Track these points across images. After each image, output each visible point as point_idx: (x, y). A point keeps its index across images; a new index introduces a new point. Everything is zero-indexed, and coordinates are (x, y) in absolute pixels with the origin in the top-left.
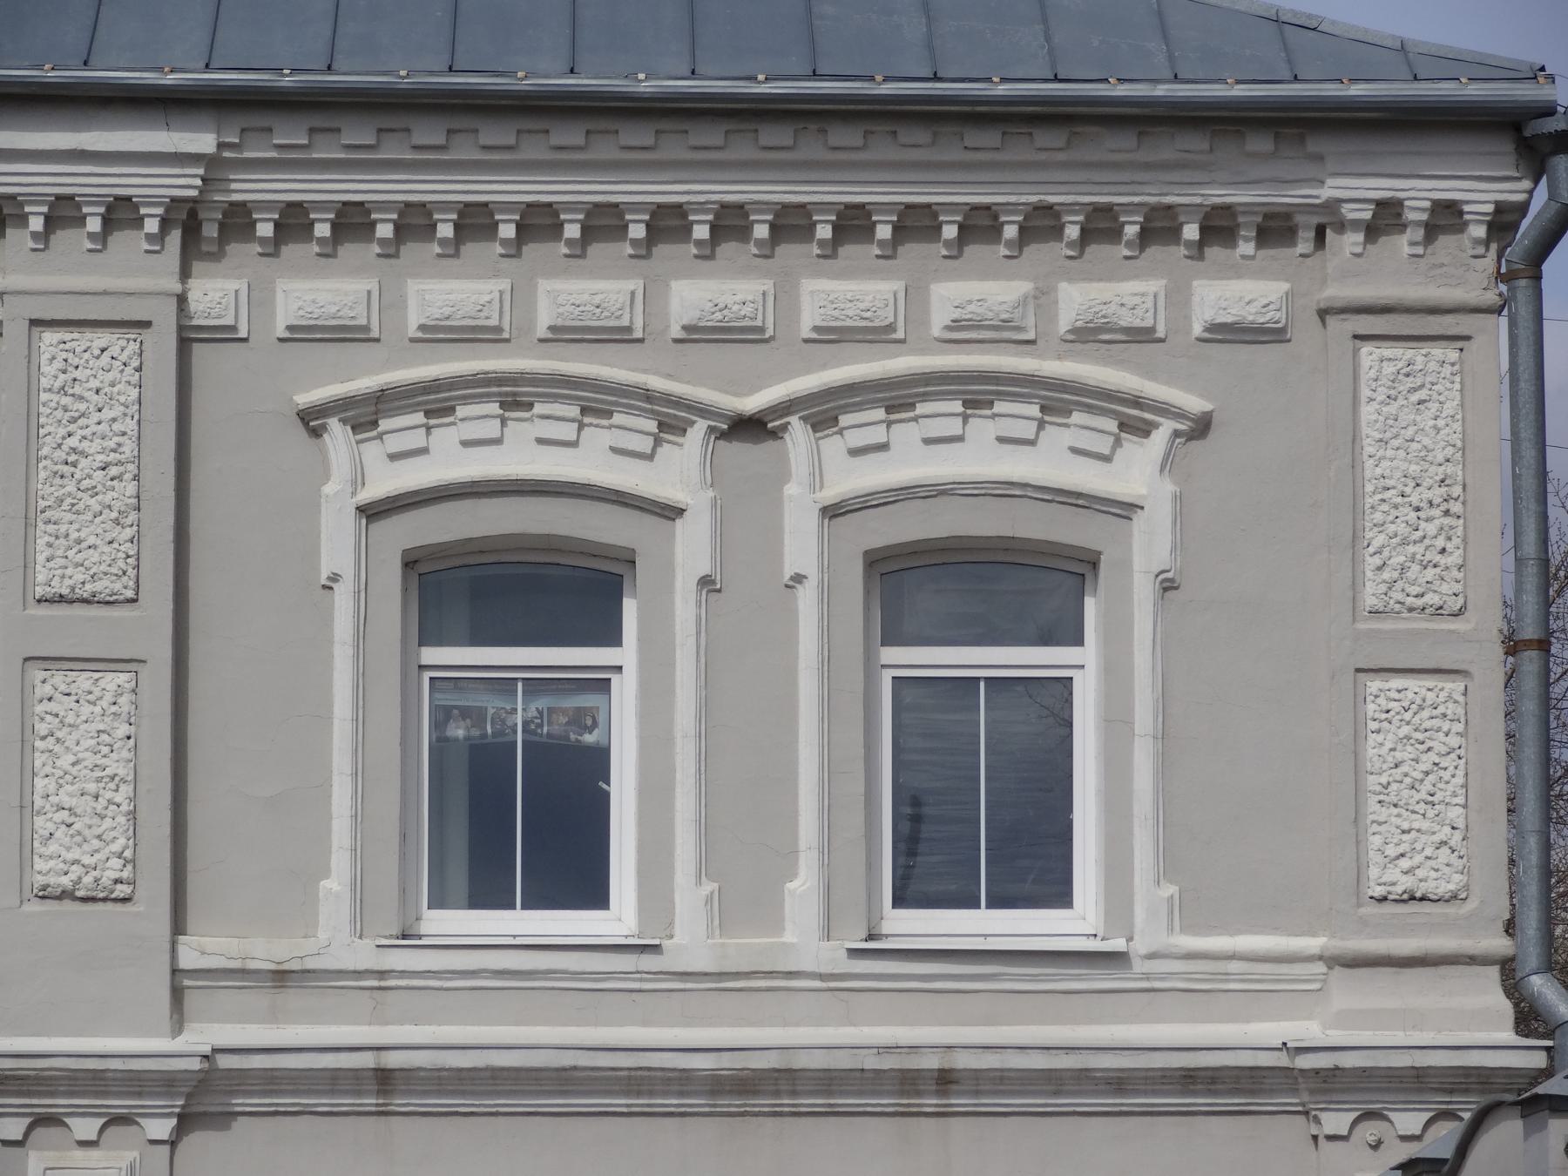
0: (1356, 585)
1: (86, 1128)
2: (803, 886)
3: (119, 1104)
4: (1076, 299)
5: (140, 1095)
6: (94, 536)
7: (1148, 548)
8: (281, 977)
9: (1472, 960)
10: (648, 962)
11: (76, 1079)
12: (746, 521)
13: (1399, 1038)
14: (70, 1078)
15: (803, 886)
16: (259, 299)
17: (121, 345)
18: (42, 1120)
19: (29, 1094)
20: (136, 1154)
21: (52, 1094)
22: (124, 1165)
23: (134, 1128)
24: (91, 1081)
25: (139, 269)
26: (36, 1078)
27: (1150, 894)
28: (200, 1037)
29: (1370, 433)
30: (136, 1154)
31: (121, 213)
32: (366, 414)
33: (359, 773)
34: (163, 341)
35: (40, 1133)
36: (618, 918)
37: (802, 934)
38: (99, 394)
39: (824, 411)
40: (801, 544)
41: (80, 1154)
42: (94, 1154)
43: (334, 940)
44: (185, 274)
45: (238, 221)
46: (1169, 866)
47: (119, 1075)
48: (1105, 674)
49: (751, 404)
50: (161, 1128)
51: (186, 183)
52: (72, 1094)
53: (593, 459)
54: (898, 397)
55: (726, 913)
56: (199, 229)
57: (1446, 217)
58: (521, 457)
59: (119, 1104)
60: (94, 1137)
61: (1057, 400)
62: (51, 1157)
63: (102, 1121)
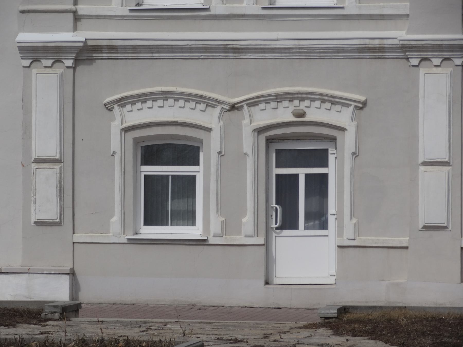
1: (437, 61)
3: (446, 54)
5: (452, 51)
11: (434, 47)
14: (432, 47)
18: (424, 59)
19: (420, 51)
20: (451, 69)
21: (427, 51)
22: (448, 72)
23: (451, 62)
24: (438, 47)
26: (422, 47)
30: (451, 69)
35: (423, 63)
41: (435, 69)
42: (439, 69)
47: (447, 46)
52: (433, 51)
59: (446, 54)
60: (439, 64)
62: (426, 70)
63: (441, 59)
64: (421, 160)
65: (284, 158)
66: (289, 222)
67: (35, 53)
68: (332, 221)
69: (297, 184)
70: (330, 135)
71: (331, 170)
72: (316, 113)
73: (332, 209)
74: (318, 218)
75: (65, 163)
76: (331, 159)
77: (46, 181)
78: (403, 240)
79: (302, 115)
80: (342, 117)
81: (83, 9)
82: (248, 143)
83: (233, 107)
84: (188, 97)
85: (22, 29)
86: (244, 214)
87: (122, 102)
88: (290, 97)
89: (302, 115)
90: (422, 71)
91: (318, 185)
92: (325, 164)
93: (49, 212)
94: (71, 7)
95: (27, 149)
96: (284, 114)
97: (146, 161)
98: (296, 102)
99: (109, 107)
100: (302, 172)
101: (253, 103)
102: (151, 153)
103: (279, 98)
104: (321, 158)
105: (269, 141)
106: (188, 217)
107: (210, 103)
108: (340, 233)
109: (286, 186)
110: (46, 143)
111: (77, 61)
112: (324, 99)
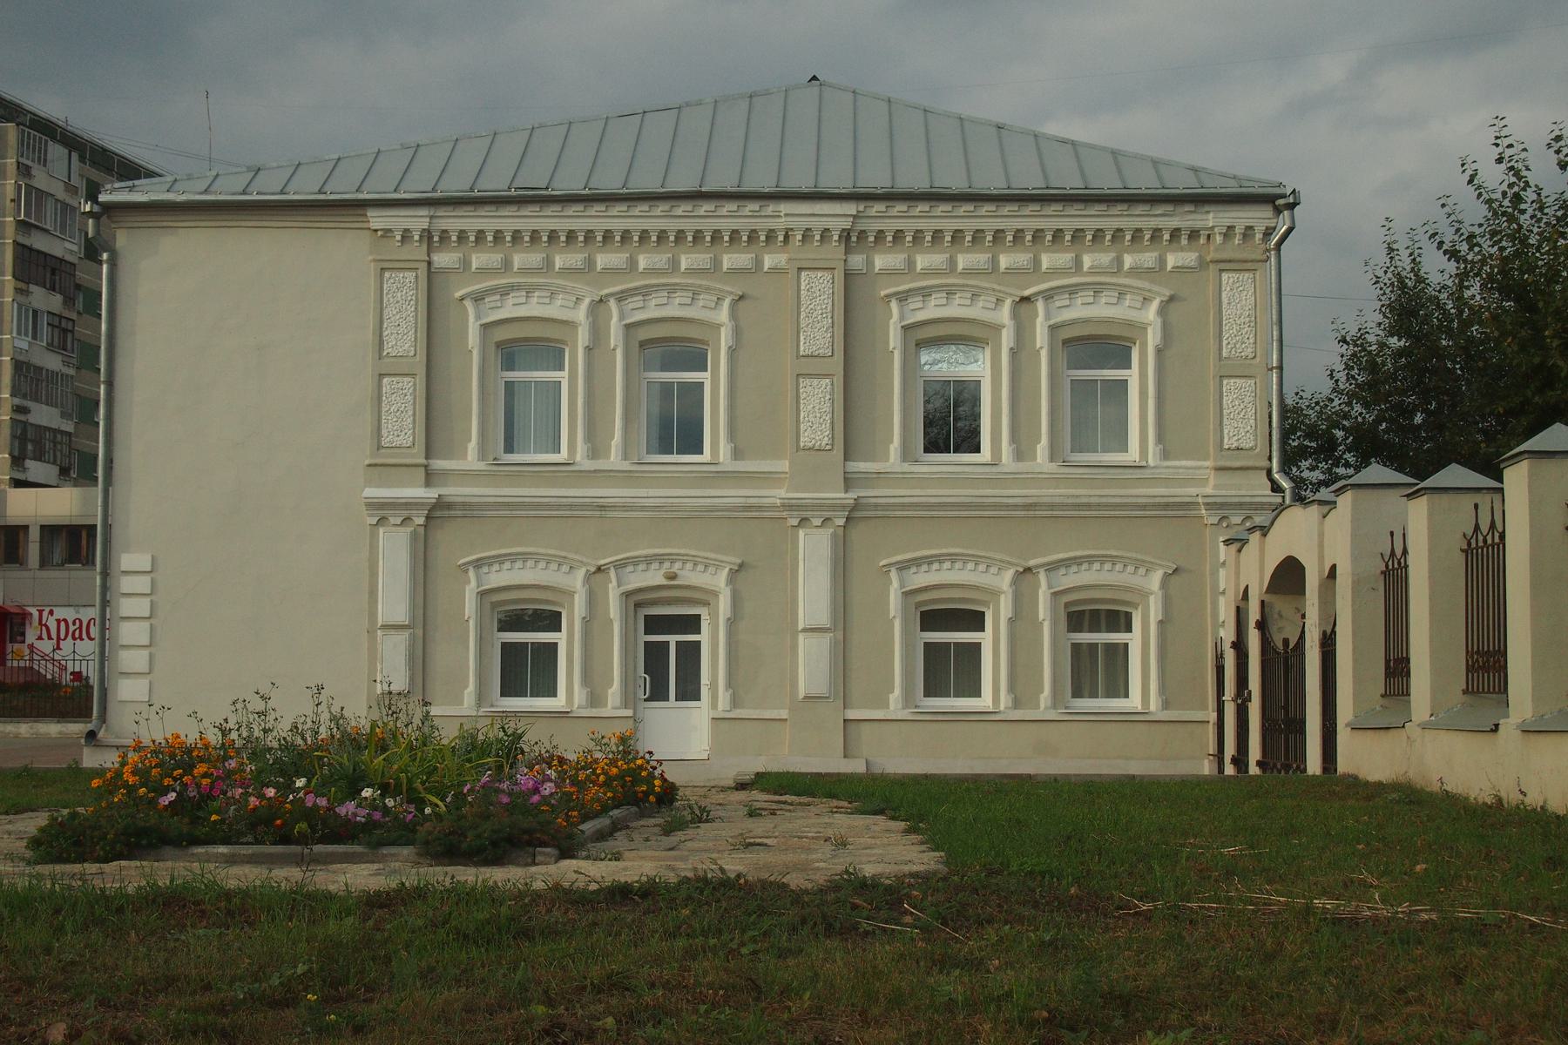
0: (1220, 349)
3: (827, 514)
6: (818, 333)
9: (1256, 468)
10: (994, 469)
13: (1233, 493)
17: (827, 275)
29: (1225, 301)
34: (839, 275)
39: (1048, 295)
44: (846, 253)
45: (862, 234)
49: (1027, 293)
51: (846, 224)
54: (1072, 290)
55: (1019, 455)
57: (1248, 231)
58: (953, 311)
64: (801, 626)
65: (653, 624)
67: (382, 510)
68: (704, 691)
71: (704, 637)
74: (689, 692)
76: (704, 625)
78: (784, 714)
81: (439, 464)
85: (369, 483)
88: (660, 558)
89: (673, 577)
91: (690, 654)
94: (423, 461)
95: (373, 615)
96: (655, 577)
97: (505, 626)
98: (667, 565)
99: (464, 569)
100: (672, 639)
103: (649, 560)
104: (693, 624)
105: (638, 605)
108: (714, 705)
109: (655, 654)
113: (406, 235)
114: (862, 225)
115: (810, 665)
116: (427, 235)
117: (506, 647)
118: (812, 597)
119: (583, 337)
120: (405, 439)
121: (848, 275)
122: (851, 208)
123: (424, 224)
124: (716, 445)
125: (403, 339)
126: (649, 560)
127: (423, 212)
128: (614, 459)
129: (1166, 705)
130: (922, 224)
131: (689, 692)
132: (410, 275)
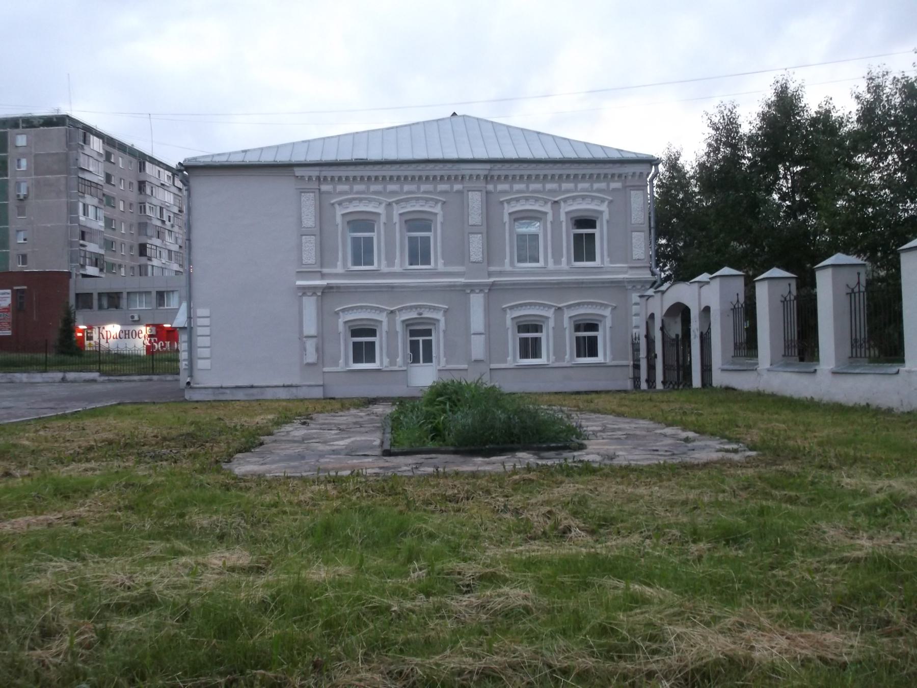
2: (564, 259)
4: (596, 186)
7: (606, 216)
8: (501, 272)
12: (556, 214)
15: (564, 259)
16: (495, 187)
17: (479, 193)
25: (481, 184)
27: (606, 259)
28: (492, 280)
31: (478, 176)
32: (509, 201)
33: (511, 247)
36: (541, 263)
37: (564, 265)
38: (475, 200)
39: (565, 200)
40: (563, 217)
43: (507, 267)
45: (492, 177)
46: (609, 256)
48: (600, 233)
50: (487, 291)
51: (486, 172)
53: (536, 207)
56: (488, 178)
61: (593, 198)
66: (416, 360)
67: (305, 290)
68: (434, 359)
69: (420, 345)
70: (435, 322)
71: (433, 338)
72: (427, 314)
73: (434, 355)
74: (428, 358)
75: (320, 337)
77: (311, 345)
78: (465, 366)
79: (421, 314)
80: (439, 316)
82: (399, 328)
83: (392, 312)
84: (372, 308)
85: (298, 279)
86: (398, 357)
87: (343, 310)
88: (416, 307)
89: (421, 314)
90: (472, 295)
91: (428, 345)
92: (431, 335)
93: (311, 357)
100: (421, 339)
101: (400, 310)
102: (355, 333)
103: (411, 308)
104: (428, 332)
106: (372, 359)
107: (381, 310)
109: (414, 346)
110: (310, 328)
111: (323, 293)
112: (430, 308)
113: (310, 178)
114: (493, 173)
115: (478, 347)
116: (318, 178)
117: (354, 344)
118: (477, 321)
119: (383, 219)
120: (312, 261)
121: (487, 192)
122: (488, 166)
123: (317, 173)
124: (437, 262)
125: (309, 220)
126: (411, 308)
127: (317, 168)
128: (397, 268)
129: (613, 359)
130: (522, 172)
131: (428, 358)
132: (312, 195)
